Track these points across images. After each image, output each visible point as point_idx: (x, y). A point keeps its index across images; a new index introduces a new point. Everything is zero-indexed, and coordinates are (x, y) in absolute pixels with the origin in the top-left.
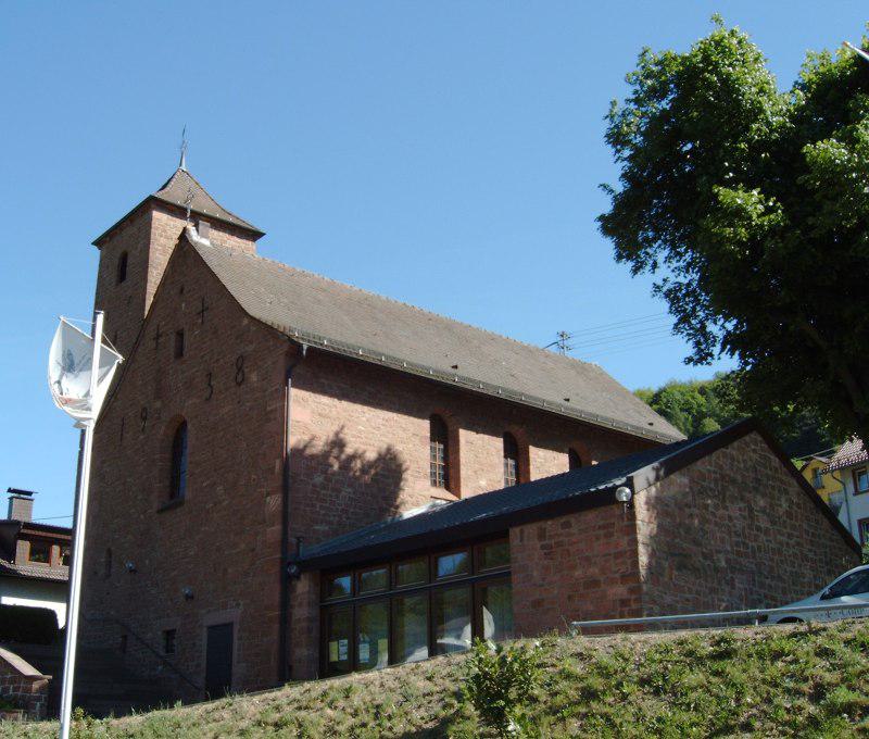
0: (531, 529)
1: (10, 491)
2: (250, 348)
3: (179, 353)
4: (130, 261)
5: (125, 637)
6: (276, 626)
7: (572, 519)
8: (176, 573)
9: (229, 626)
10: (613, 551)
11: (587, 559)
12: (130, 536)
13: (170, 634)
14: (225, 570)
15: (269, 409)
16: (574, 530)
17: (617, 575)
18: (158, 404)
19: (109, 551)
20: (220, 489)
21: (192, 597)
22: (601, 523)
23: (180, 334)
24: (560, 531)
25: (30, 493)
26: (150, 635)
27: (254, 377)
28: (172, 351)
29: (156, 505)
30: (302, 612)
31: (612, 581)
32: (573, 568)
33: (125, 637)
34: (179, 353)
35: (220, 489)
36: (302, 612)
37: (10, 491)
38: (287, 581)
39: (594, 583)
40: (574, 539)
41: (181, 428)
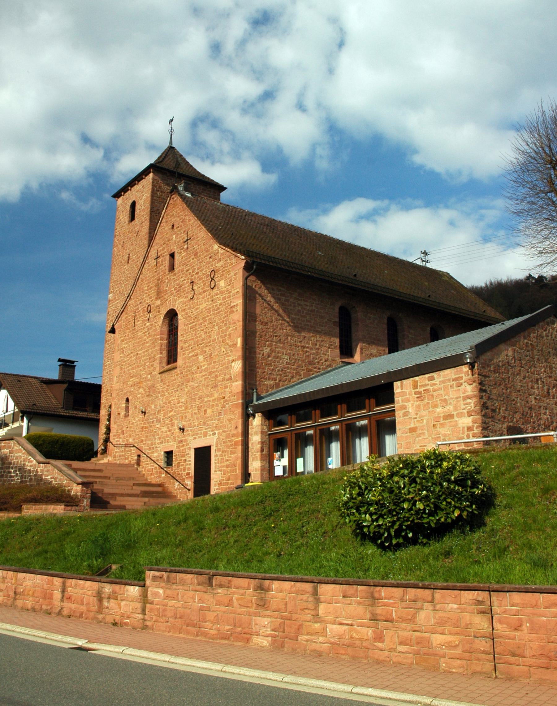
0: (408, 383)
1: (60, 360)
2: (219, 265)
3: (172, 268)
4: (138, 207)
5: (139, 456)
6: (240, 448)
7: (435, 375)
8: (172, 413)
9: (208, 448)
10: (462, 395)
11: (445, 400)
12: (141, 390)
13: (169, 455)
14: (205, 411)
15: (233, 304)
16: (437, 381)
17: (465, 411)
18: (158, 302)
19: (127, 400)
20: (201, 358)
21: (183, 429)
22: (454, 377)
23: (172, 255)
24: (427, 382)
25: (73, 362)
26: (156, 454)
27: (222, 283)
28: (167, 268)
29: (158, 370)
30: (255, 439)
31: (460, 415)
32: (436, 406)
33: (139, 456)
34: (172, 268)
35: (201, 358)
36: (255, 439)
37: (60, 360)
38: (247, 417)
39: (451, 416)
40: (435, 387)
41: (172, 315)
